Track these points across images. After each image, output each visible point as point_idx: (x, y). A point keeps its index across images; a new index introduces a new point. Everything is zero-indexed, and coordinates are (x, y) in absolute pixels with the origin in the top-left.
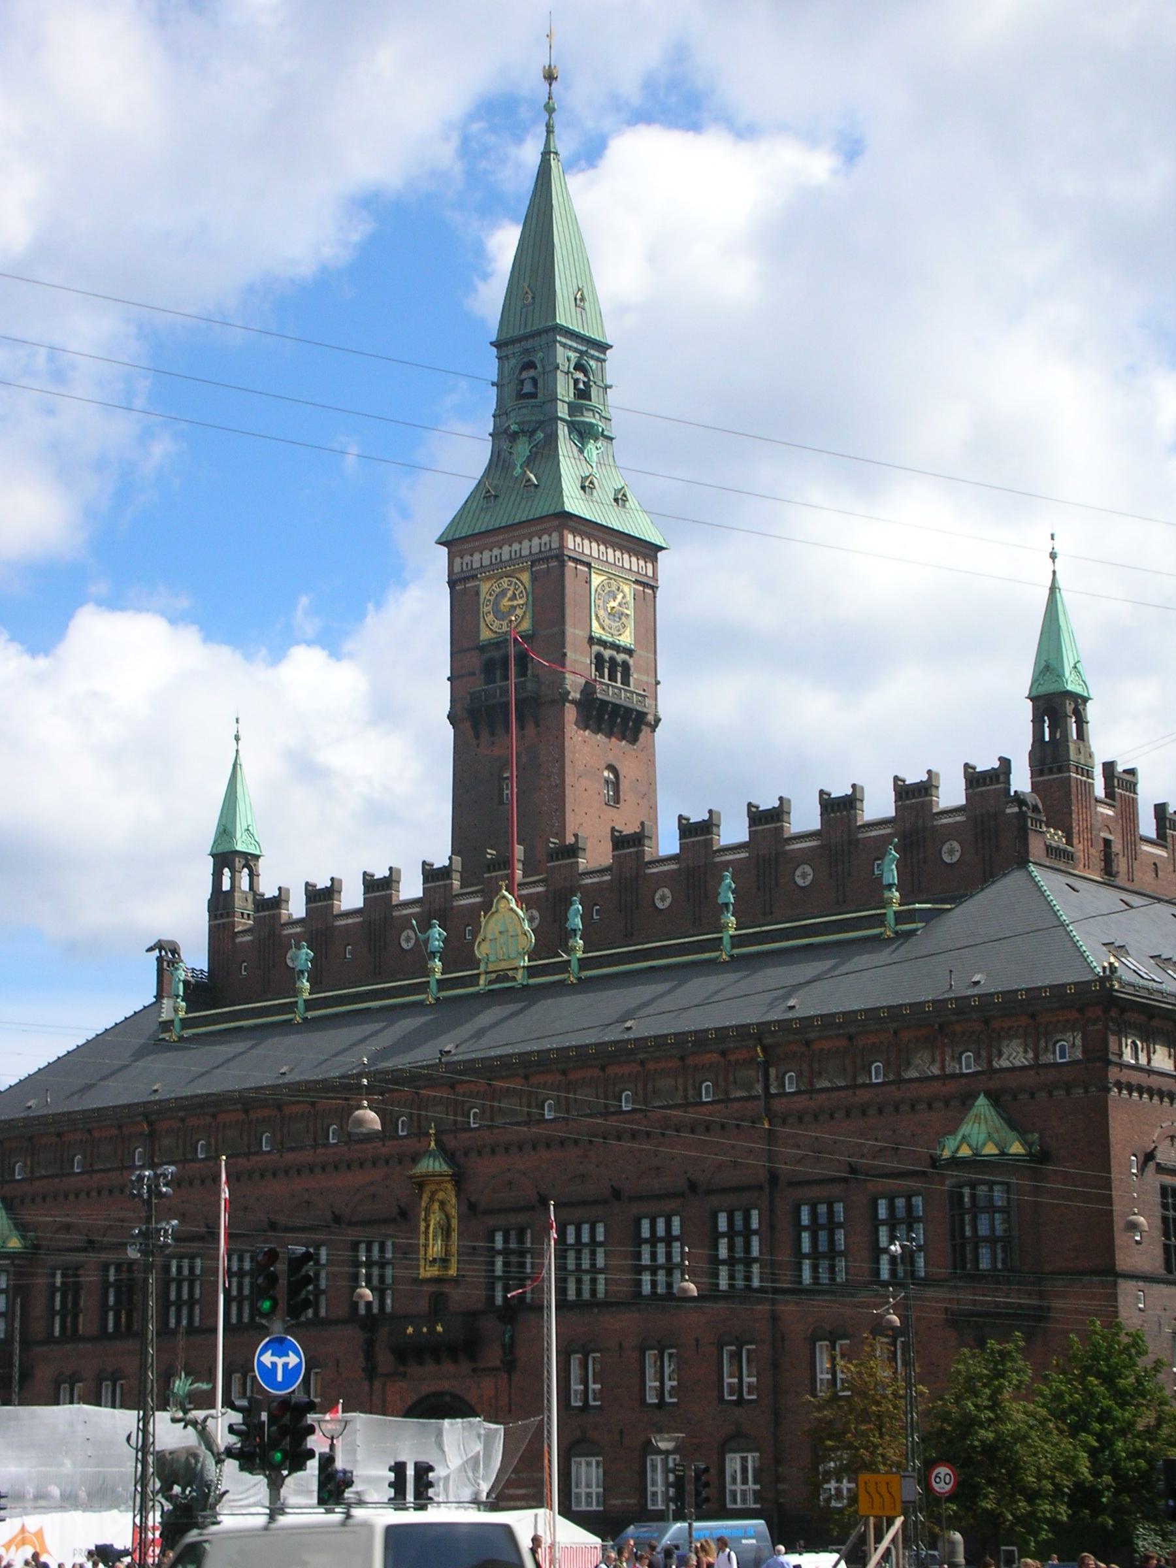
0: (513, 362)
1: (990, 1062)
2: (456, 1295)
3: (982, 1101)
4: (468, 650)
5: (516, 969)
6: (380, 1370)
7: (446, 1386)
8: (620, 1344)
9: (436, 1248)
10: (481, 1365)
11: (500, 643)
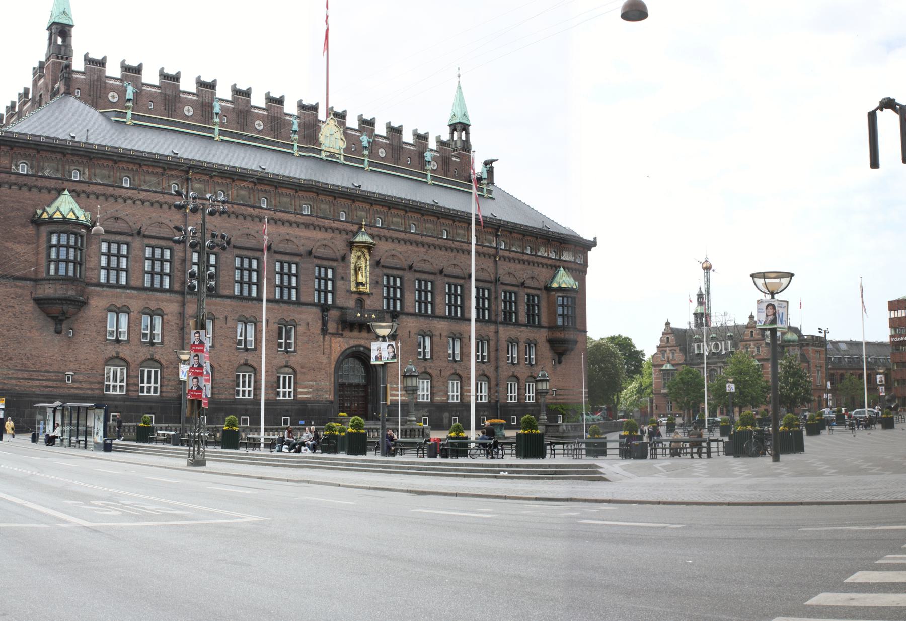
1: (560, 257)
2: (368, 302)
3: (562, 269)
5: (340, 154)
6: (329, 331)
8: (441, 334)
9: (361, 279)
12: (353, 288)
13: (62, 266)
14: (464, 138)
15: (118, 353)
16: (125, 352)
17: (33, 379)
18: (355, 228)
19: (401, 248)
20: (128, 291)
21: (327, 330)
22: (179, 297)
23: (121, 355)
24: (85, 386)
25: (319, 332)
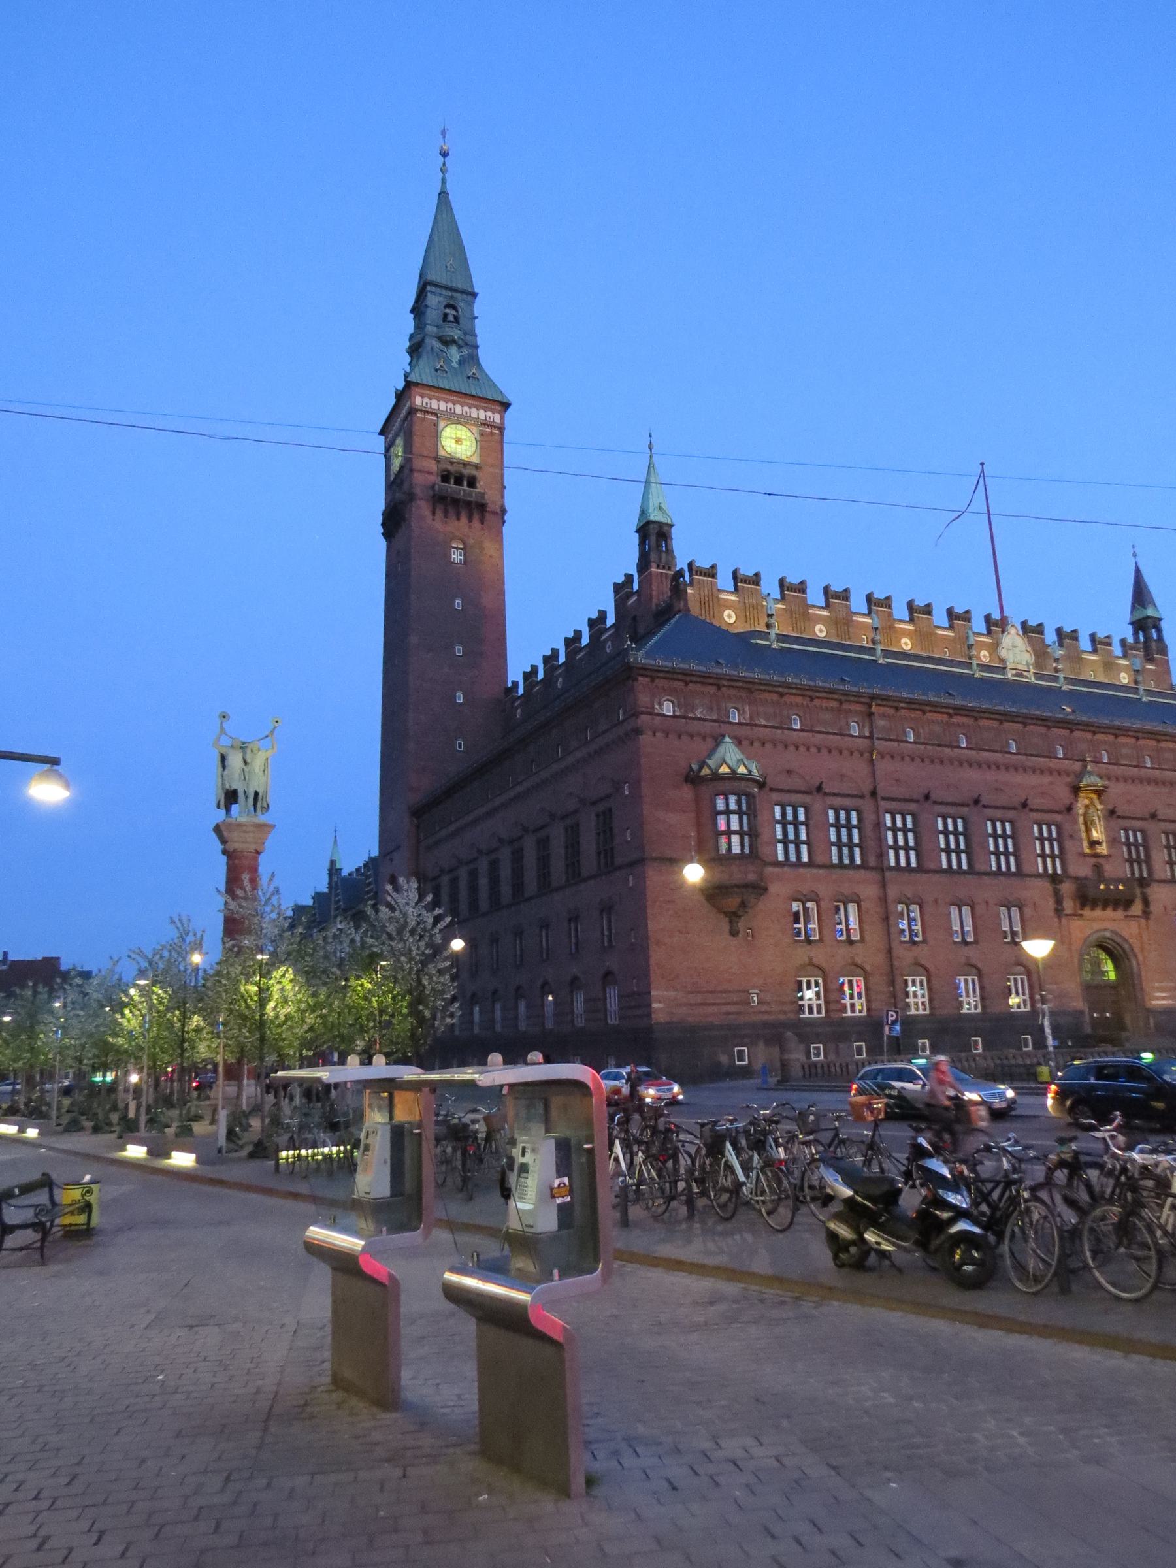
0: (441, 299)
4: (430, 457)
7: (1107, 925)
9: (1095, 835)
10: (1130, 913)
11: (453, 461)
12: (1087, 851)
13: (735, 839)
14: (1155, 636)
15: (810, 958)
16: (819, 955)
17: (709, 1004)
18: (1077, 766)
19: (1137, 789)
20: (815, 871)
21: (1063, 910)
22: (874, 876)
23: (815, 961)
24: (774, 1008)
25: (1052, 913)
